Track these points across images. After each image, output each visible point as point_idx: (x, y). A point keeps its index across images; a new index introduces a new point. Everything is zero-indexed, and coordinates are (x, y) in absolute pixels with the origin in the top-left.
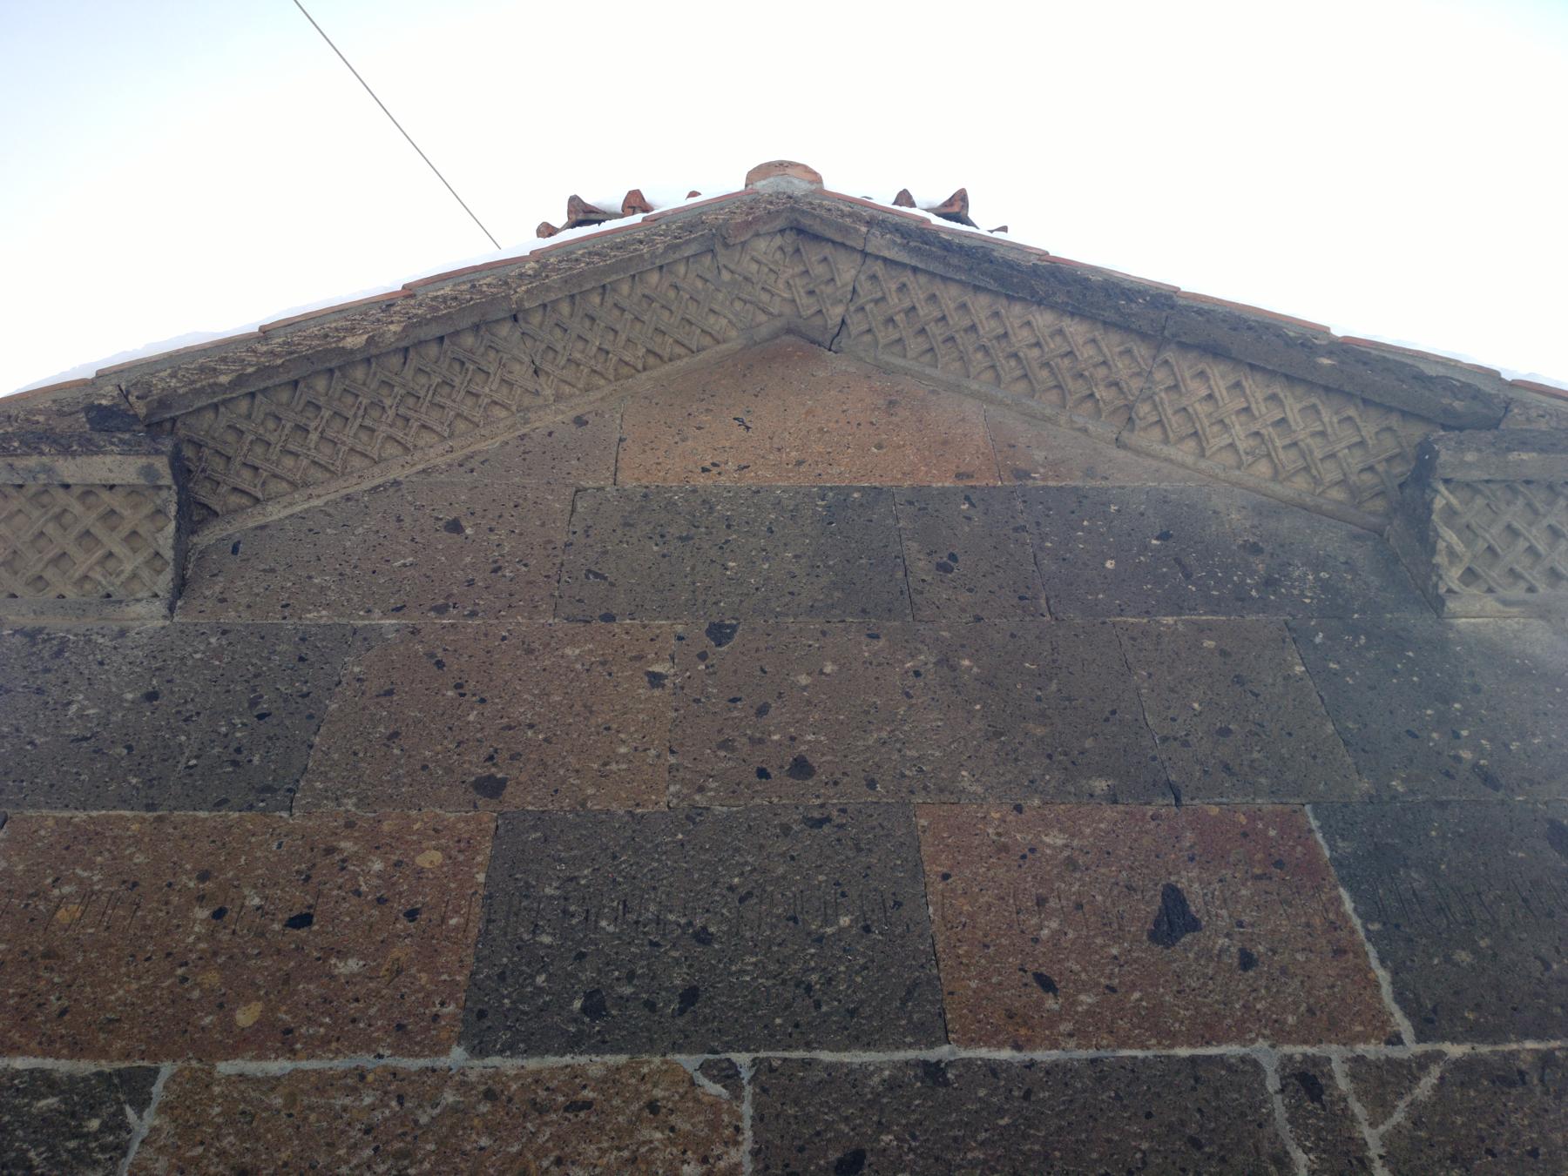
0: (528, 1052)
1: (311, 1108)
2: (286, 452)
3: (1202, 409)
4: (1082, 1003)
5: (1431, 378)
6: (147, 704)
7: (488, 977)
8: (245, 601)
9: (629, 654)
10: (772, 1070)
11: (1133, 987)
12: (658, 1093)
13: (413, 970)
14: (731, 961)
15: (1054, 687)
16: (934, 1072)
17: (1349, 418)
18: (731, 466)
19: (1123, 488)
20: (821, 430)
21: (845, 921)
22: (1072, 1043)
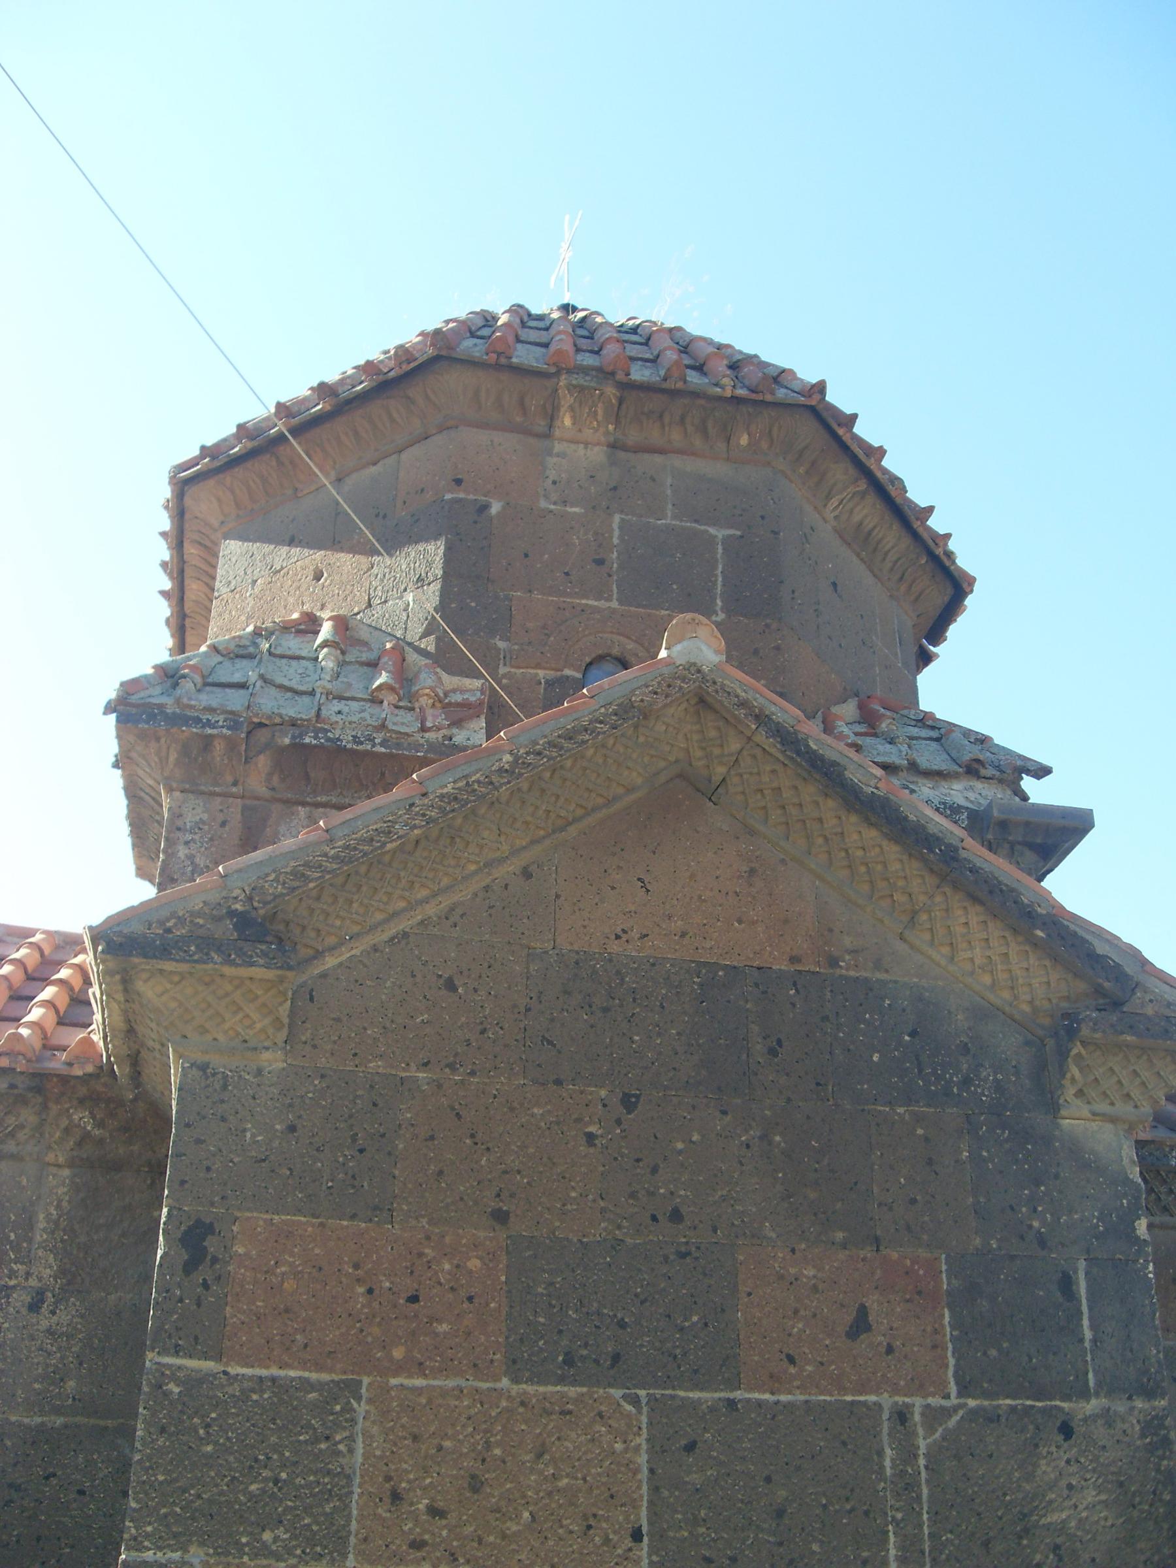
0: (538, 1383)
1: (440, 1406)
2: (338, 916)
3: (960, 930)
4: (806, 1371)
5: (1098, 955)
6: (291, 1135)
7: (515, 1340)
8: (329, 1047)
10: (656, 1400)
12: (603, 1408)
14: (637, 1339)
15: (826, 1162)
16: (731, 1404)
17: (1045, 966)
18: (635, 934)
19: (896, 982)
21: (695, 1319)
22: (798, 1392)
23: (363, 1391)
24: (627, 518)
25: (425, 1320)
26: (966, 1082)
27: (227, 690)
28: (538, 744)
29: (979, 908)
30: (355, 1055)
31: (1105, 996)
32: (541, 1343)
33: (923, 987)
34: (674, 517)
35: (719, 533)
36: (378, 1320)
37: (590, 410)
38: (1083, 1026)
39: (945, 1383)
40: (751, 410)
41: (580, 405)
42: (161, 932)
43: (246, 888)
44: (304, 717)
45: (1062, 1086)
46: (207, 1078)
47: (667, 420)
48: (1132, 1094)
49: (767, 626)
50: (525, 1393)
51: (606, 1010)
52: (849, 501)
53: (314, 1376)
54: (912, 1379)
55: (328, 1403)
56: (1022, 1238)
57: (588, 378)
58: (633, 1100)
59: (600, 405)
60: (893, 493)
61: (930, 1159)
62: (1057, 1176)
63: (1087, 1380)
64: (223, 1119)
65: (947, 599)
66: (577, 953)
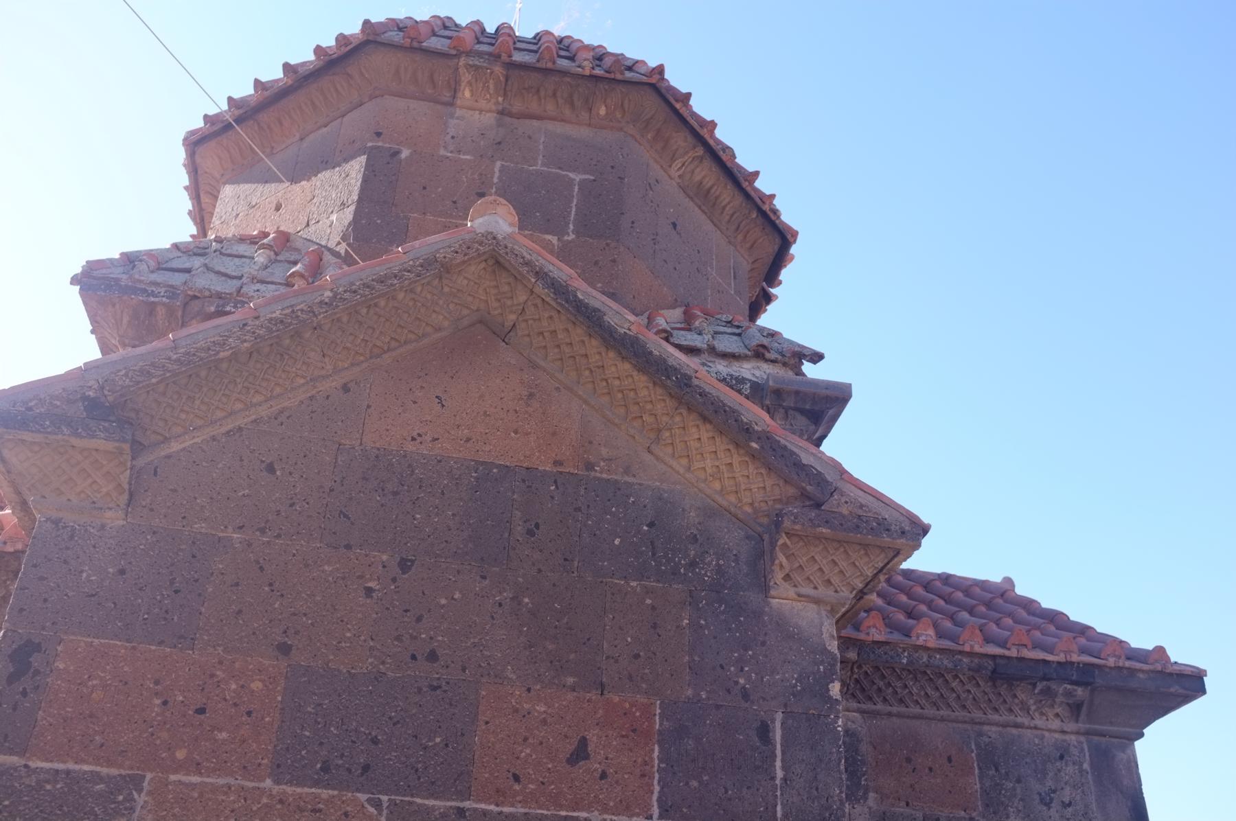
0: (298, 785)
1: (210, 799)
2: (182, 411)
3: (694, 444)
4: (529, 788)
7: (281, 749)
9: (357, 574)
10: (396, 804)
11: (553, 783)
12: (349, 809)
13: (250, 741)
14: (386, 754)
15: (565, 620)
16: (461, 812)
17: (761, 473)
18: (428, 438)
19: (640, 484)
20: (485, 412)
21: (438, 740)
22: (520, 805)
23: (145, 784)
24: (506, 164)
25: (208, 728)
26: (693, 564)
27: (176, 274)
28: (355, 285)
29: (709, 427)
30: (184, 518)
31: (809, 498)
32: (303, 752)
33: (663, 490)
34: (543, 165)
35: (577, 177)
36: (168, 726)
37: (484, 84)
38: (785, 518)
39: (650, 806)
40: (607, 87)
41: (476, 81)
42: (24, 409)
43: (100, 380)
44: (227, 292)
45: (773, 571)
46: (58, 530)
47: (542, 93)
48: (832, 580)
49: (608, 245)
50: (285, 792)
51: (395, 493)
52: (688, 165)
53: (104, 771)
54: (621, 801)
55: (112, 793)
56: (729, 691)
57: (481, 60)
58: (409, 564)
59: (491, 81)
60: (724, 157)
61: (655, 624)
62: (763, 643)
63: (776, 811)
64: (65, 562)
65: (776, 248)
66: (378, 449)
